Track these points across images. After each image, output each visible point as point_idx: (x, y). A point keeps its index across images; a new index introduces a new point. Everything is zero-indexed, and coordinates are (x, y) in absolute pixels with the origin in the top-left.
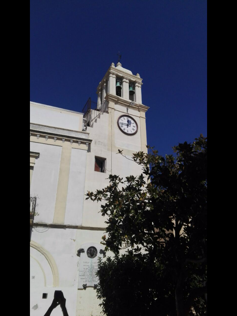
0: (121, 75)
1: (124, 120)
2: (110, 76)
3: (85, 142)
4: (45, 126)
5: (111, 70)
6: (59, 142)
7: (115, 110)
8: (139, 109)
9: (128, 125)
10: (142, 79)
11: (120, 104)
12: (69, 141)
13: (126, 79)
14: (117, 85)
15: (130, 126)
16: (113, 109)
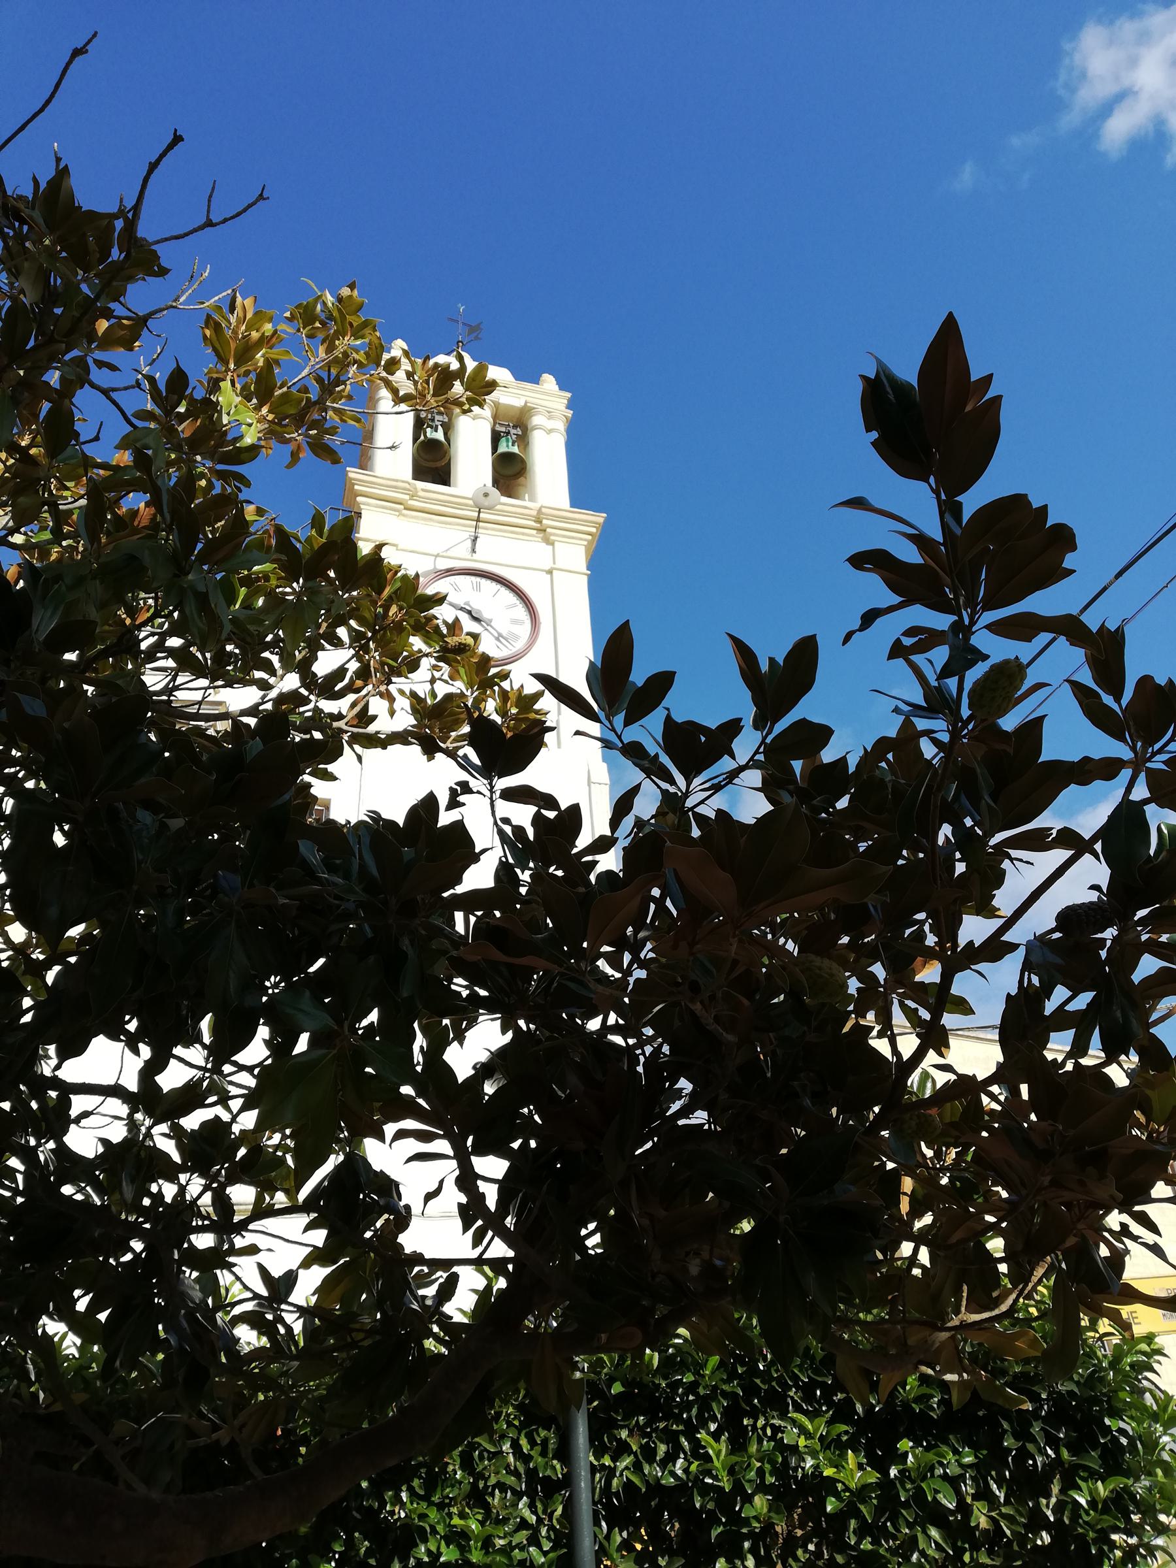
10: (569, 395)
11: (431, 520)
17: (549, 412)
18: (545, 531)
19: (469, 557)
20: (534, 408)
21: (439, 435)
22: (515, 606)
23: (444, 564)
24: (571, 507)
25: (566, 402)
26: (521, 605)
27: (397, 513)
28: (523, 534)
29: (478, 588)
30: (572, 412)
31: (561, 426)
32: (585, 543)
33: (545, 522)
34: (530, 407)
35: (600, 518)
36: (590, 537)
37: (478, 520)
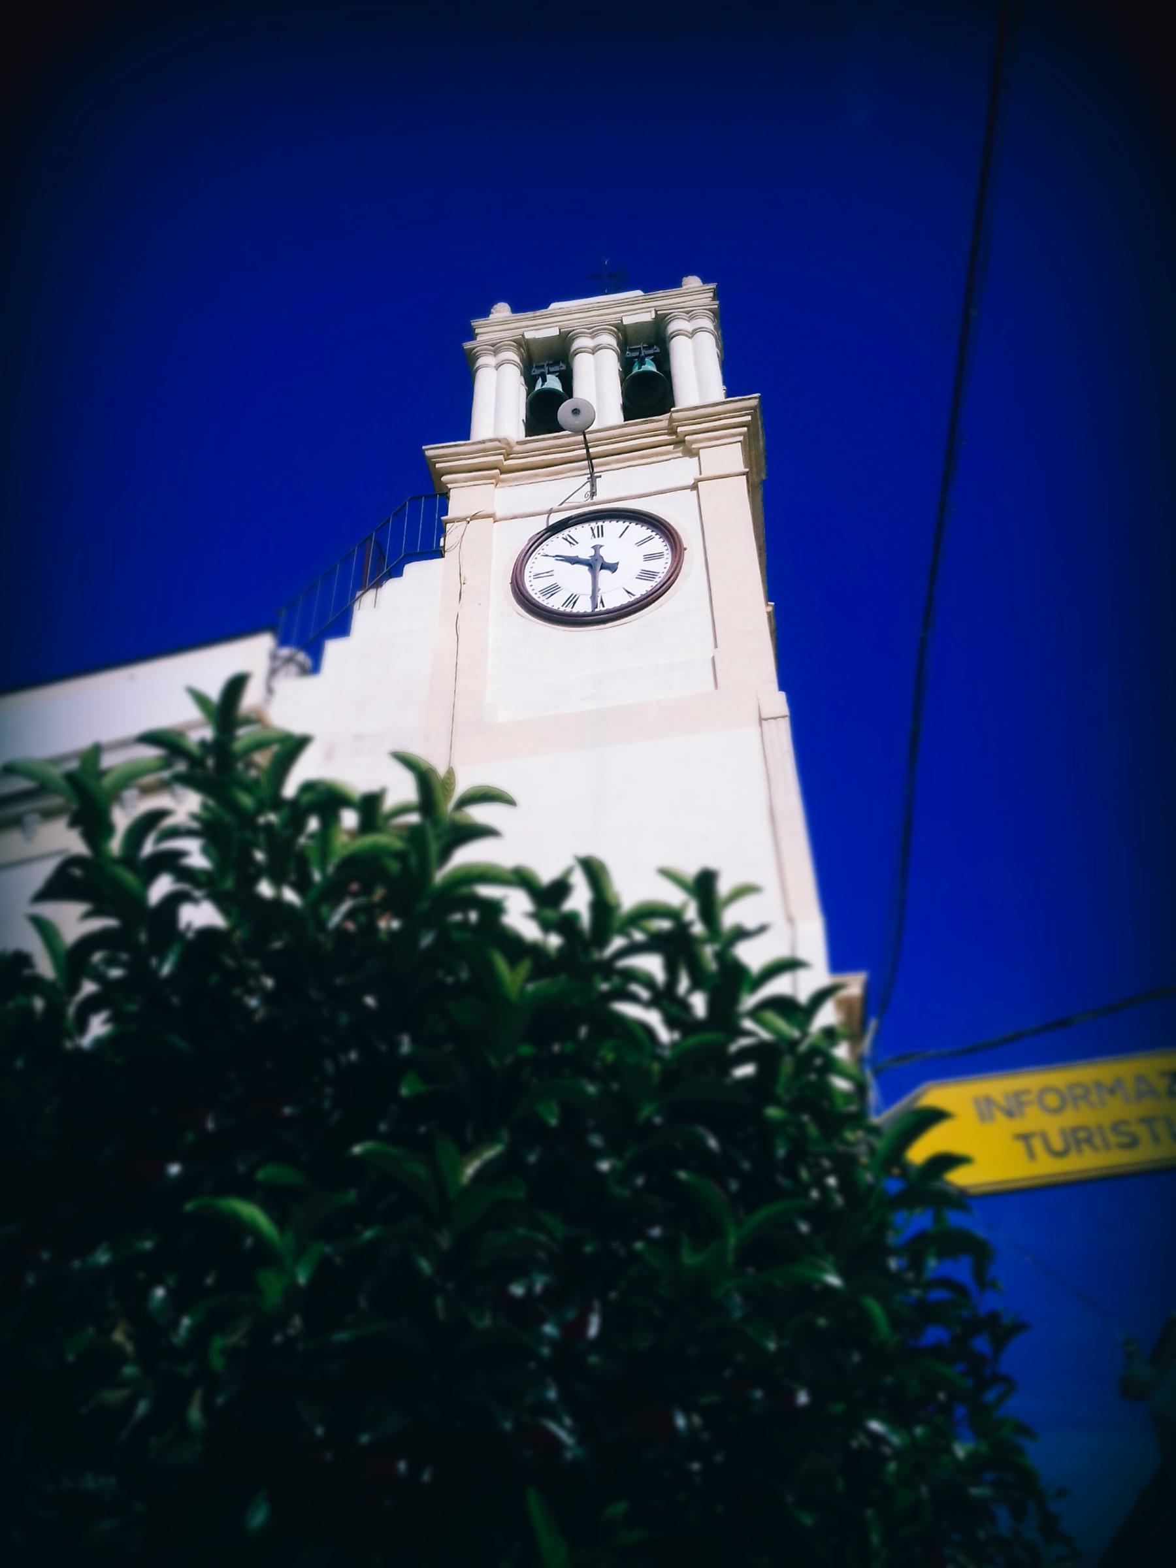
0: (554, 332)
2: (478, 369)
5: (479, 338)
8: (680, 442)
10: (713, 286)
11: (536, 475)
13: (593, 336)
14: (538, 387)
16: (474, 517)
17: (688, 313)
18: (684, 441)
19: (589, 501)
21: (554, 383)
22: (650, 538)
23: (555, 518)
25: (711, 294)
26: (658, 536)
27: (493, 481)
28: (657, 454)
29: (601, 532)
30: (717, 302)
31: (708, 323)
32: (741, 438)
33: (679, 429)
35: (753, 400)
36: (745, 429)
37: (589, 457)
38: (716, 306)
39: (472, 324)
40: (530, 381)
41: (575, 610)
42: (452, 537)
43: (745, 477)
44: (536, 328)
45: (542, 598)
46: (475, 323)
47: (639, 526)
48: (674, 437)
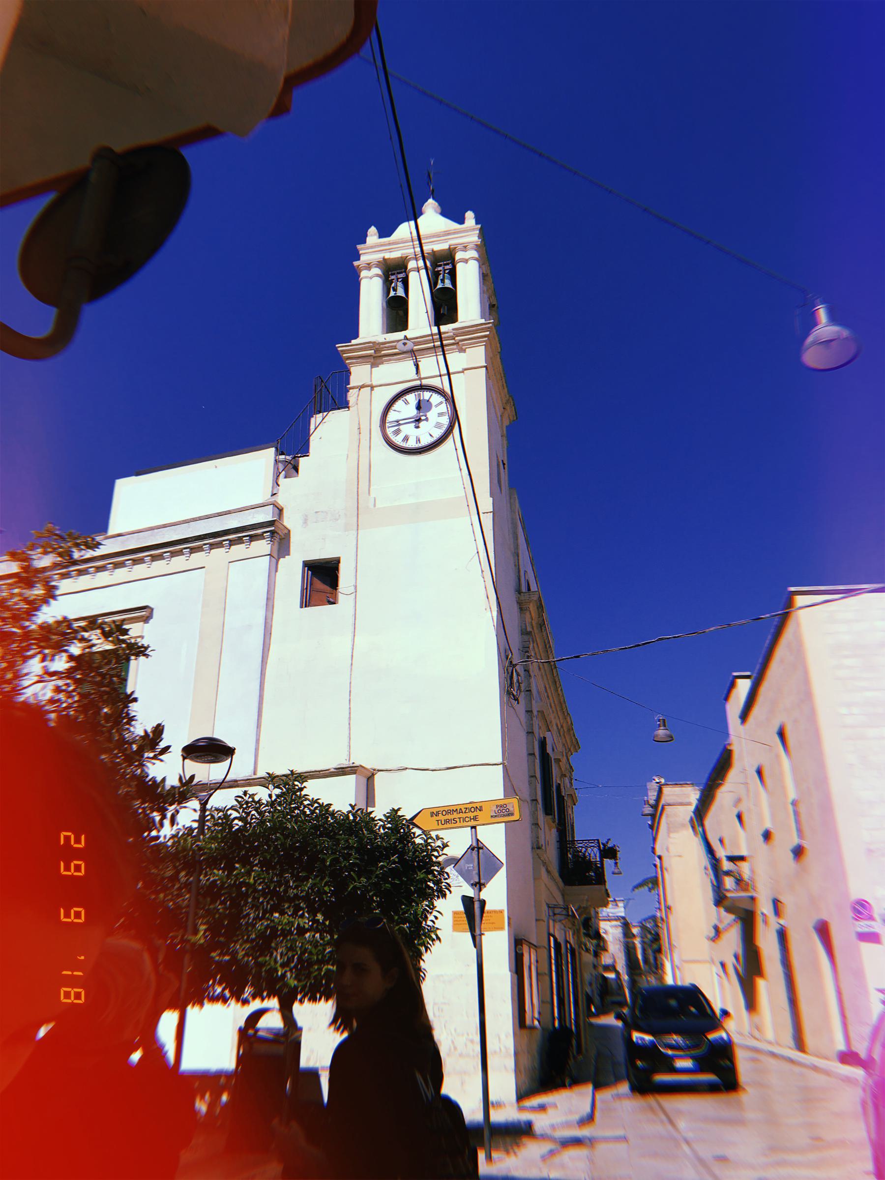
1: (406, 409)
3: (260, 531)
4: (165, 526)
5: (363, 258)
6: (198, 558)
7: (372, 387)
9: (418, 420)
10: (479, 226)
11: (390, 360)
12: (219, 545)
14: (392, 294)
15: (427, 419)
20: (457, 247)
21: (401, 292)
22: (441, 403)
24: (482, 318)
25: (478, 232)
34: (453, 248)
38: (479, 243)
39: (358, 248)
40: (387, 284)
41: (407, 446)
42: (352, 396)
43: (485, 368)
44: (390, 250)
45: (394, 436)
46: (359, 247)
47: (437, 395)
48: (454, 341)
